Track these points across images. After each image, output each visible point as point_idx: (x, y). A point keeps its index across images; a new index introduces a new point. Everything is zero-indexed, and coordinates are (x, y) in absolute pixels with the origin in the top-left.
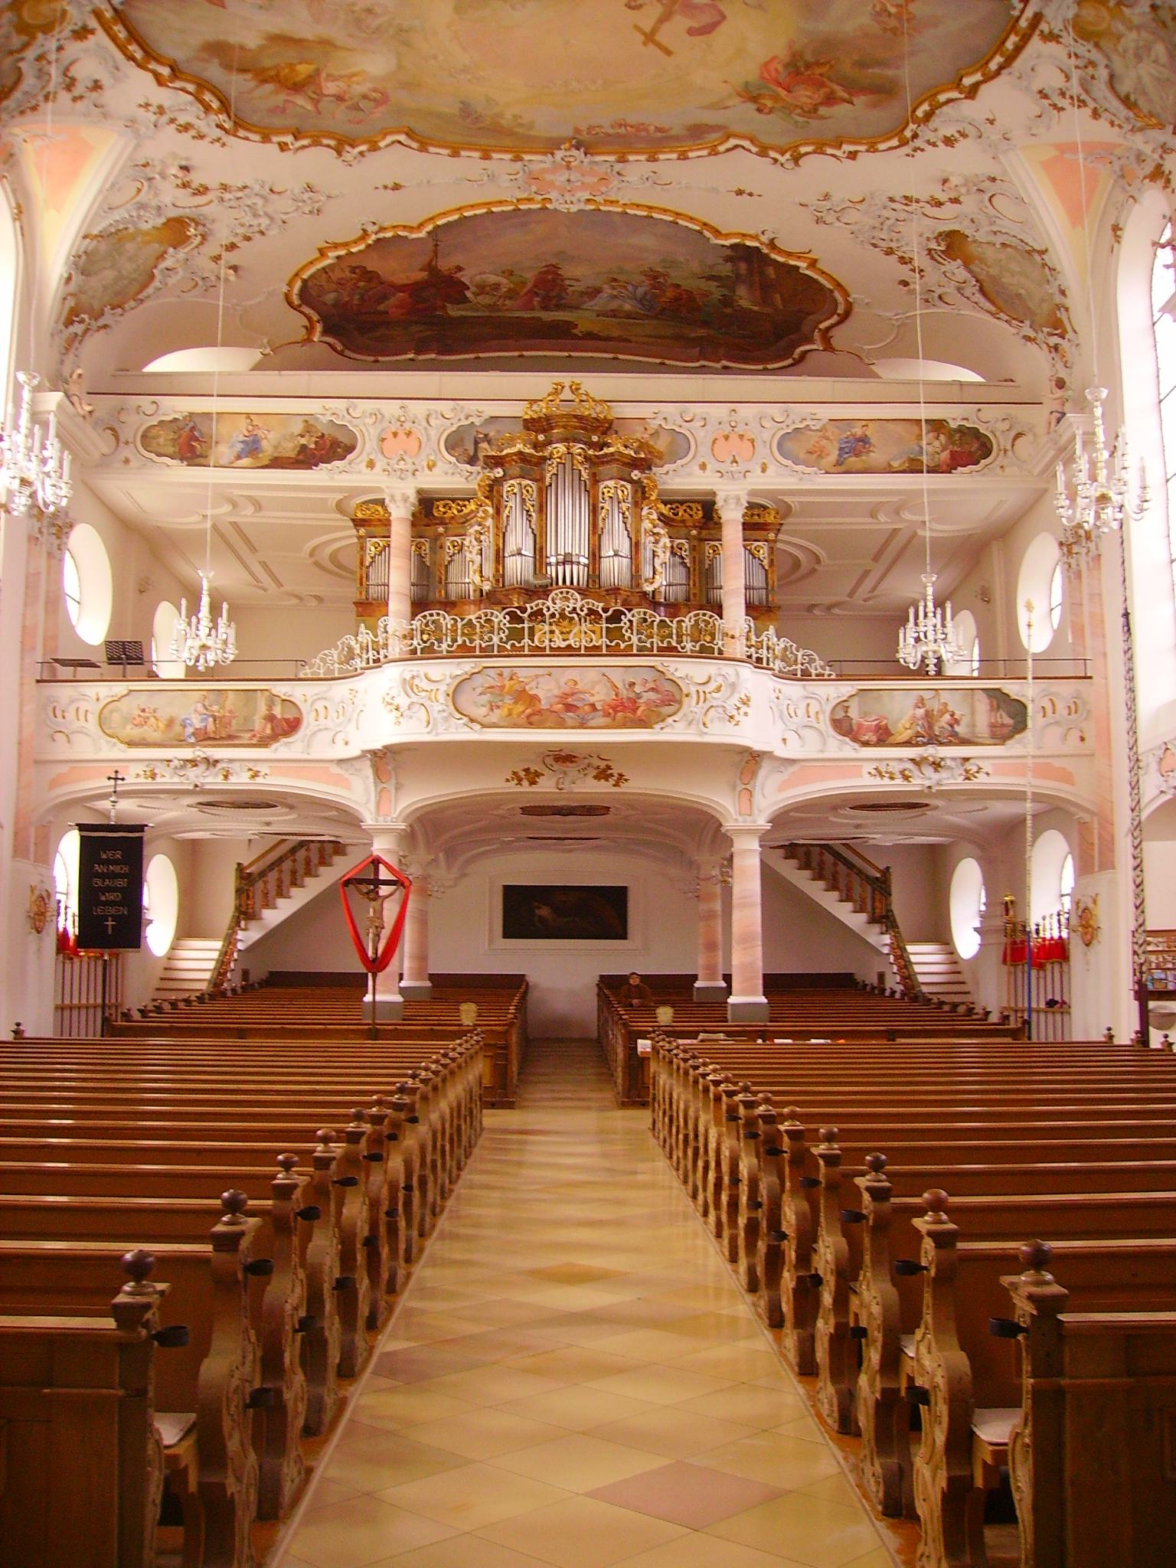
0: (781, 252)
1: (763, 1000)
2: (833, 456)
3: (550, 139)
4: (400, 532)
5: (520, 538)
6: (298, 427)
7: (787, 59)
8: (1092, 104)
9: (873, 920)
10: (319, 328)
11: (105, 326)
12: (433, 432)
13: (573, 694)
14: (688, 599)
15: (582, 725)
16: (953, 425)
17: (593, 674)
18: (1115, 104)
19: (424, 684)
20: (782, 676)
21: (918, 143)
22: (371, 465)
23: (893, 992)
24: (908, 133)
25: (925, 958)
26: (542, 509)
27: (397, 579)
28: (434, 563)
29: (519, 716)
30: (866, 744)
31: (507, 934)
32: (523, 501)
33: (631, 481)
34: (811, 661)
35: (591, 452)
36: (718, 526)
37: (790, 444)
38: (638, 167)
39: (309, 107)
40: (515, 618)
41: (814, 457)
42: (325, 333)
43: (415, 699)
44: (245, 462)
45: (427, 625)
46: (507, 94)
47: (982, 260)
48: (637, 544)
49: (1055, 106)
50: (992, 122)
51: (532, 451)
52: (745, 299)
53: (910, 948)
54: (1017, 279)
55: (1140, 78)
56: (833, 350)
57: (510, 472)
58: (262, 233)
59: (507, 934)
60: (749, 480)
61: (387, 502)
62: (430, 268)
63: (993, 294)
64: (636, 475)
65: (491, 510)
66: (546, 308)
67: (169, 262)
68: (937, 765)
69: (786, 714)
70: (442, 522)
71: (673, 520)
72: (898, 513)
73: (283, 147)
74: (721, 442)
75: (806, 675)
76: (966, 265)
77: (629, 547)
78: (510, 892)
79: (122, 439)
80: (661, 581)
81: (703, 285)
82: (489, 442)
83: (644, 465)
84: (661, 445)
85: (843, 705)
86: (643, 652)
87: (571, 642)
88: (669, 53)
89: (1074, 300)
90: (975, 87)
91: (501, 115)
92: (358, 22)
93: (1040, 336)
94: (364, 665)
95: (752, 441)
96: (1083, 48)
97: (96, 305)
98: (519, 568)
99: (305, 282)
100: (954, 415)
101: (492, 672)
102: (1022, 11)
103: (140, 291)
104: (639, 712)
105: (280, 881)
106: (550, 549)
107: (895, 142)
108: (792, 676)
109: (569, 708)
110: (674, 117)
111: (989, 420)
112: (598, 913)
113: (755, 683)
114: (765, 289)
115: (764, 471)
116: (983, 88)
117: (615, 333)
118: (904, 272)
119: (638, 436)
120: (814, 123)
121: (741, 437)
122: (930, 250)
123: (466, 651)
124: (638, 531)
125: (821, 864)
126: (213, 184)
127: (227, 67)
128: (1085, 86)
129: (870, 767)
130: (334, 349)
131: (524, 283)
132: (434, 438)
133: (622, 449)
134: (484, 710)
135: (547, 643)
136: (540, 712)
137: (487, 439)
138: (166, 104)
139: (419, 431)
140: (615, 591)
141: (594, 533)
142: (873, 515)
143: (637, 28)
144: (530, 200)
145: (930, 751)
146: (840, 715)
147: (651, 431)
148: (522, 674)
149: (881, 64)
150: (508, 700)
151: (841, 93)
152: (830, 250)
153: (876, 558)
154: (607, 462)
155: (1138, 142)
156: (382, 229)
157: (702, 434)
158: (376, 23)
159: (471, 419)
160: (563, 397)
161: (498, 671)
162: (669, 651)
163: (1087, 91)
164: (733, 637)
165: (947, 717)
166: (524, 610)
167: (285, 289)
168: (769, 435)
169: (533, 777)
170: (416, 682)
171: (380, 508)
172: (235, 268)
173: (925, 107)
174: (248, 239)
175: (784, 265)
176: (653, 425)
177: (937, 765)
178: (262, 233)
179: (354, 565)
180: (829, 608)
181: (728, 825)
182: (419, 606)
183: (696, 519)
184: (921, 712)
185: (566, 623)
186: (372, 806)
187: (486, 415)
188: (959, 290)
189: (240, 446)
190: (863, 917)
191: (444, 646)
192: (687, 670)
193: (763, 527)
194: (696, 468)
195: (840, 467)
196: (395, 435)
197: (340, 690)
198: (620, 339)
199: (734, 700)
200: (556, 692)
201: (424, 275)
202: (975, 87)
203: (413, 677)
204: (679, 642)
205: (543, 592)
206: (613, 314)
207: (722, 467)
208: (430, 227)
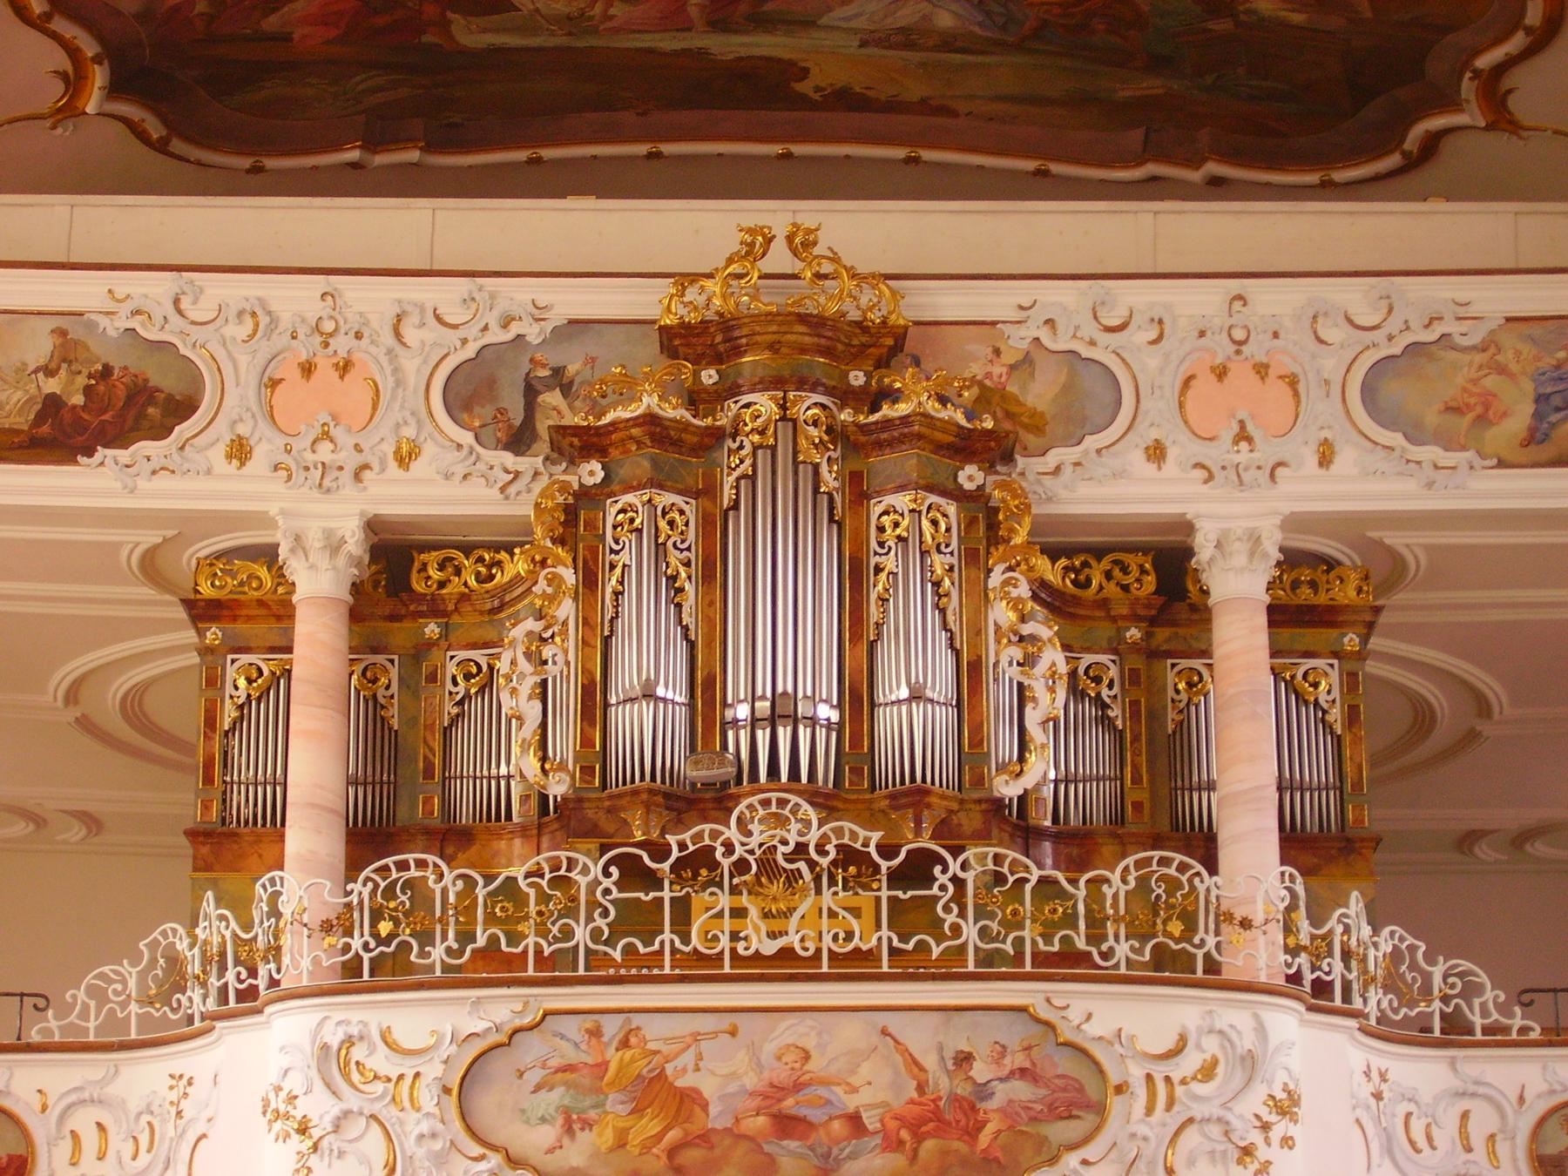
2: (1520, 418)
4: (318, 640)
5: (648, 658)
6: (38, 346)
10: (99, 77)
12: (413, 367)
13: (798, 1087)
14: (1119, 819)
17: (852, 1031)
19: (382, 1061)
20: (1385, 1031)
22: (240, 451)
26: (712, 571)
27: (314, 767)
28: (412, 722)
29: (646, 1148)
32: (660, 549)
33: (958, 495)
34: (1471, 990)
35: (845, 416)
37: (1397, 387)
40: (634, 873)
41: (1466, 421)
42: (116, 90)
43: (353, 1101)
45: (390, 892)
48: (976, 667)
51: (682, 414)
61: (283, 552)
64: (970, 476)
65: (569, 576)
66: (718, 24)
70: (435, 609)
71: (1076, 601)
74: (1205, 384)
75: (1455, 1031)
77: (960, 675)
80: (1041, 768)
82: (566, 389)
83: (995, 450)
84: (1039, 393)
86: (992, 966)
87: (793, 940)
94: (211, 1006)
95: (1293, 382)
98: (647, 727)
101: (571, 1026)
104: (985, 1138)
106: (736, 682)
108: (1416, 1034)
109: (787, 1125)
113: (1311, 1051)
115: (1325, 460)
117: (915, 90)
119: (976, 369)
121: (1262, 370)
123: (494, 967)
124: (977, 632)
132: (414, 380)
133: (932, 407)
134: (547, 1134)
135: (725, 942)
136: (705, 1138)
137: (560, 380)
139: (372, 358)
140: (914, 797)
141: (856, 636)
147: (1009, 358)
148: (655, 1030)
150: (616, 1105)
154: (891, 444)
159: (515, 328)
160: (767, 265)
161: (588, 1022)
162: (1067, 963)
164: (1246, 924)
168: (1335, 363)
170: (358, 1053)
171: (263, 572)
176: (1018, 340)
179: (189, 724)
180: (1521, 839)
182: (368, 838)
183: (1141, 595)
185: (776, 888)
187: (558, 316)
191: (437, 953)
192: (1121, 1020)
193: (1328, 617)
194: (1136, 459)
196: (308, 369)
197: (144, 1077)
198: (925, 107)
199: (1254, 1103)
200: (751, 1081)
203: (349, 1042)
204: (1095, 938)
205: (715, 800)
206: (906, 39)
207: (1215, 454)
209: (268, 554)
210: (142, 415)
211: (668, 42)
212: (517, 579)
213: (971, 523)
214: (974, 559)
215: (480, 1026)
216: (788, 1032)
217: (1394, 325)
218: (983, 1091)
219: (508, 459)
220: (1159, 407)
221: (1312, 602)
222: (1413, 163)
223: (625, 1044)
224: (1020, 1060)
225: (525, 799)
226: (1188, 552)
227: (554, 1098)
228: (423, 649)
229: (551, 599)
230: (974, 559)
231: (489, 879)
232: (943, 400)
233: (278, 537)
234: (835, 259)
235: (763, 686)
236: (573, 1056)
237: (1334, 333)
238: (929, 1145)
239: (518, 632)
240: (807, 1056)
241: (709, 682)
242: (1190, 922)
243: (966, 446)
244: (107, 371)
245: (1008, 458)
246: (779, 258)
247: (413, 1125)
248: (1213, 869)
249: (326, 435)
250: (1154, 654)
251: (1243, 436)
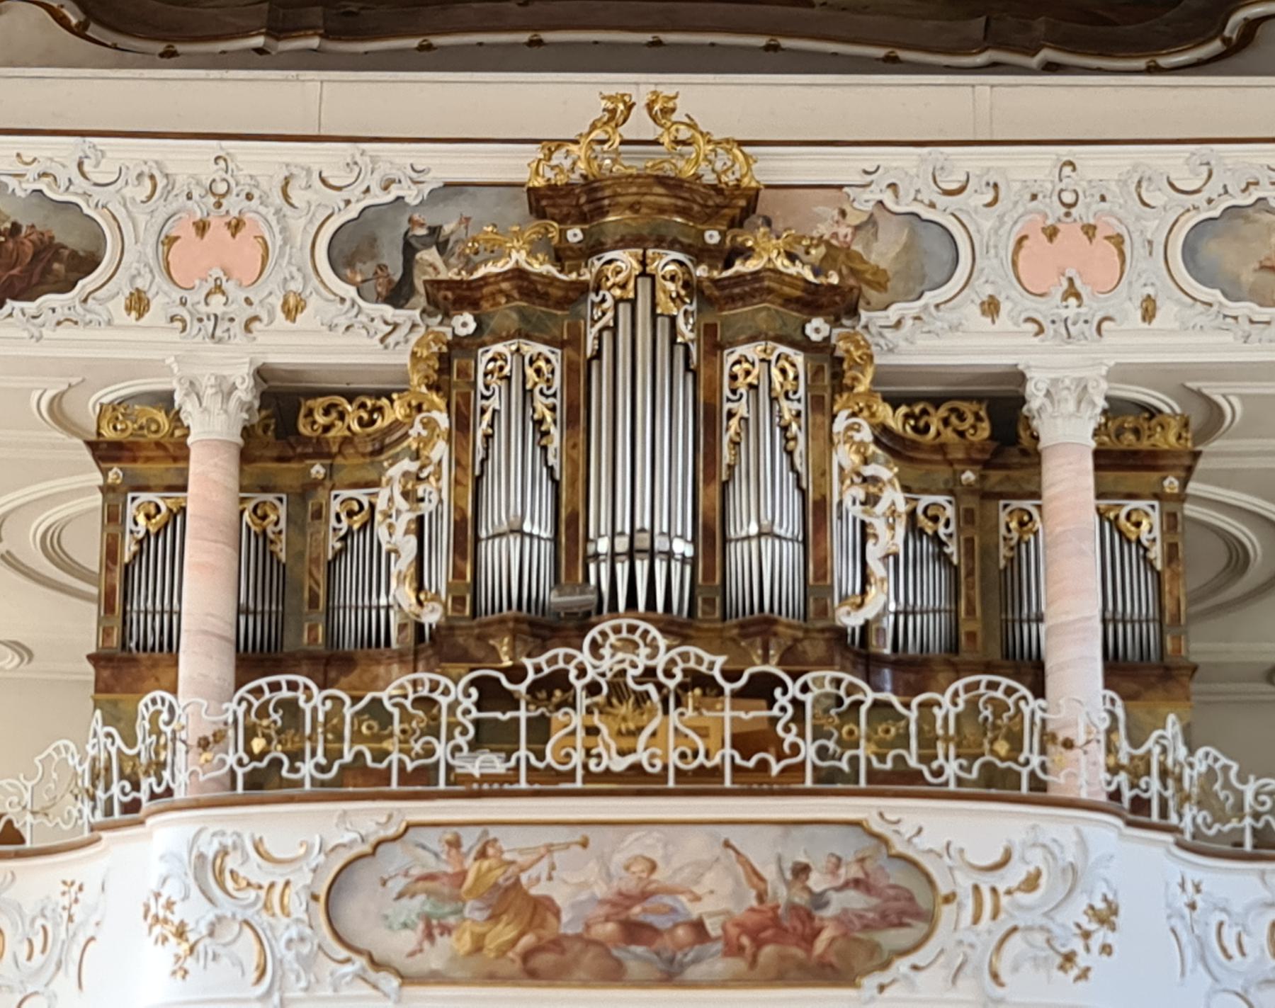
4: (211, 481)
12: (300, 226)
13: (644, 896)
14: (953, 646)
17: (697, 845)
19: (254, 870)
20: (1198, 847)
22: (138, 303)
26: (576, 415)
27: (205, 598)
29: (502, 952)
32: (527, 394)
33: (805, 345)
35: (701, 271)
36: (1032, 457)
40: (490, 694)
43: (226, 907)
45: (263, 712)
48: (822, 506)
51: (550, 269)
57: (493, 324)
60: (1108, 339)
61: (178, 398)
64: (817, 328)
65: (442, 420)
70: (320, 450)
71: (915, 445)
80: (879, 600)
82: (442, 248)
83: (842, 305)
84: (882, 253)
87: (642, 757)
94: (99, 817)
95: (1118, 241)
98: (516, 560)
101: (434, 839)
104: (820, 944)
109: (634, 931)
115: (1149, 313)
119: (824, 230)
121: (1089, 230)
124: (824, 473)
130: (62, 21)
132: (301, 239)
133: (781, 263)
134: (410, 939)
135: (578, 758)
136: (557, 944)
140: (760, 627)
141: (710, 477)
147: (853, 219)
148: (511, 844)
150: (474, 912)
154: (743, 299)
157: (987, 225)
159: (394, 192)
160: (627, 131)
161: (449, 834)
162: (901, 781)
164: (1068, 744)
166: (516, 674)
168: (1160, 224)
170: (231, 863)
171: (161, 417)
176: (864, 202)
179: (90, 555)
185: (626, 709)
187: (435, 179)
191: (307, 769)
192: (948, 833)
193: (1149, 461)
196: (202, 228)
199: (1076, 912)
200: (601, 891)
203: (224, 852)
205: (571, 626)
209: (165, 400)
210: (47, 270)
212: (396, 424)
213: (818, 371)
214: (820, 406)
215: (347, 837)
216: (637, 844)
217: (1213, 189)
218: (819, 901)
219: (388, 311)
220: (994, 267)
221: (1134, 451)
223: (482, 854)
224: (855, 872)
225: (402, 627)
226: (1023, 401)
227: (418, 904)
229: (427, 442)
230: (820, 406)
231: (355, 700)
232: (792, 257)
233: (174, 385)
234: (692, 126)
235: (623, 524)
236: (433, 866)
238: (768, 951)
239: (395, 471)
240: (653, 867)
241: (573, 519)
242: (1016, 742)
244: (16, 228)
245: (853, 312)
247: (285, 930)
248: (1039, 692)
249: (219, 289)
250: (988, 496)
251: (1072, 292)
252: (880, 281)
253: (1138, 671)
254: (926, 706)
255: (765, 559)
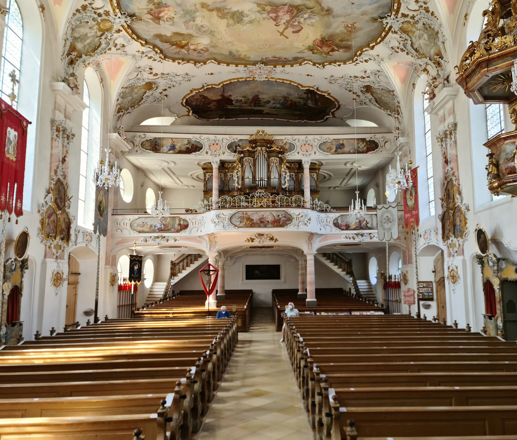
0: (320, 91)
1: (315, 300)
2: (334, 149)
3: (255, 61)
4: (215, 172)
5: (248, 175)
7: (321, 39)
8: (406, 51)
9: (347, 274)
10: (191, 112)
11: (129, 112)
14: (294, 189)
15: (265, 226)
16: (368, 140)
17: (268, 213)
18: (413, 51)
19: (222, 216)
21: (357, 62)
23: (353, 295)
24: (355, 59)
25: (362, 284)
26: (254, 165)
27: (215, 185)
30: (343, 230)
31: (247, 279)
33: (279, 157)
34: (328, 207)
37: (322, 146)
38: (279, 68)
39: (186, 52)
41: (329, 150)
43: (220, 220)
44: (171, 152)
46: (242, 49)
47: (376, 93)
48: (281, 175)
49: (396, 51)
50: (378, 56)
52: (310, 103)
53: (358, 281)
54: (386, 98)
55: (420, 44)
56: (335, 117)
58: (174, 86)
59: (247, 279)
62: (222, 95)
63: (379, 102)
64: (280, 156)
66: (255, 106)
67: (147, 94)
68: (362, 235)
69: (321, 222)
70: (227, 168)
72: (352, 164)
73: (179, 63)
76: (372, 95)
78: (247, 267)
79: (135, 145)
80: (287, 185)
81: (298, 100)
83: (282, 153)
84: (287, 147)
85: (337, 219)
86: (281, 206)
88: (287, 38)
89: (402, 105)
90: (373, 47)
91: (241, 55)
92: (199, 29)
93: (393, 114)
95: (312, 145)
96: (404, 36)
97: (126, 107)
98: (248, 181)
99: (187, 99)
100: (368, 137)
101: (241, 213)
102: (386, 26)
103: (139, 102)
105: (183, 266)
107: (351, 62)
108: (322, 211)
109: (262, 222)
110: (290, 55)
111: (378, 138)
112: (271, 272)
113: (313, 214)
114: (316, 101)
115: (315, 153)
116: (376, 46)
117: (275, 113)
118: (355, 96)
120: (329, 57)
121: (309, 144)
122: (361, 91)
123: (233, 207)
124: (281, 171)
125: (333, 258)
126: (159, 73)
127: (162, 41)
128: (404, 45)
129: (344, 236)
131: (249, 100)
132: (224, 146)
134: (239, 223)
136: (254, 223)
138: (144, 51)
139: (220, 143)
140: (274, 188)
142: (345, 164)
143: (278, 31)
144: (250, 77)
145: (361, 231)
146: (336, 222)
148: (249, 213)
149: (348, 40)
150: (245, 220)
151: (336, 48)
152: (335, 91)
153: (347, 175)
155: (419, 61)
156: (208, 85)
158: (205, 29)
162: (288, 206)
163: (405, 47)
165: (365, 222)
167: (181, 101)
168: (316, 144)
169: (252, 240)
172: (166, 96)
173: (359, 52)
174: (170, 88)
175: (321, 95)
176: (285, 141)
177: (362, 235)
178: (174, 86)
180: (335, 188)
181: (305, 252)
182: (222, 192)
183: (298, 166)
184: (358, 221)
186: (208, 248)
188: (370, 101)
189: (169, 147)
190: (345, 273)
191: (227, 206)
192: (294, 212)
193: (315, 169)
194: (296, 153)
195: (336, 152)
196: (213, 144)
198: (276, 114)
199: (306, 219)
201: (220, 97)
202: (373, 47)
204: (291, 203)
206: (274, 108)
207: (305, 153)
208: (222, 85)
209: (210, 163)
211: (250, 108)
214: (280, 164)
218: (280, 219)
220: (299, 148)
222: (325, 121)
227: (239, 220)
228: (226, 173)
230: (280, 164)
237: (316, 141)
242: (300, 202)
243: (280, 153)
246: (261, 133)
247: (226, 222)
248: (303, 197)
250: (298, 173)
251: (307, 151)
252: (287, 150)
253: (313, 192)
254: (291, 199)
255: (274, 181)
